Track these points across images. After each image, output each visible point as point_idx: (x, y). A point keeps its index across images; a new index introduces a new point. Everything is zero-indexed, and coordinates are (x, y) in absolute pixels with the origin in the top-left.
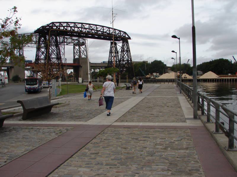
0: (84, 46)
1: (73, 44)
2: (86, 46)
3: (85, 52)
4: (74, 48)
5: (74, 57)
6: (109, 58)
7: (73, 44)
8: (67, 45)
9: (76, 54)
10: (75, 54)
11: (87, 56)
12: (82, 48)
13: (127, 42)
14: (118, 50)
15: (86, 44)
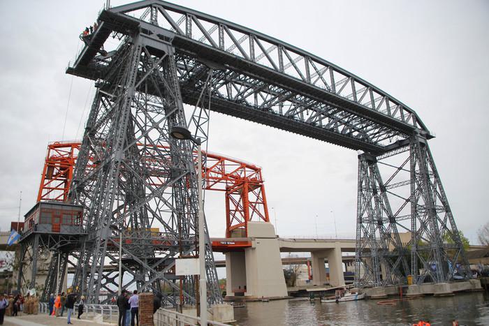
0: (257, 191)
1: (222, 186)
2: (262, 190)
3: (260, 208)
4: (228, 198)
5: (229, 223)
6: (359, 208)
7: (222, 186)
8: (208, 188)
9: (234, 216)
10: (231, 217)
11: (266, 219)
12: (252, 197)
13: (424, 145)
14: (384, 183)
15: (262, 182)
